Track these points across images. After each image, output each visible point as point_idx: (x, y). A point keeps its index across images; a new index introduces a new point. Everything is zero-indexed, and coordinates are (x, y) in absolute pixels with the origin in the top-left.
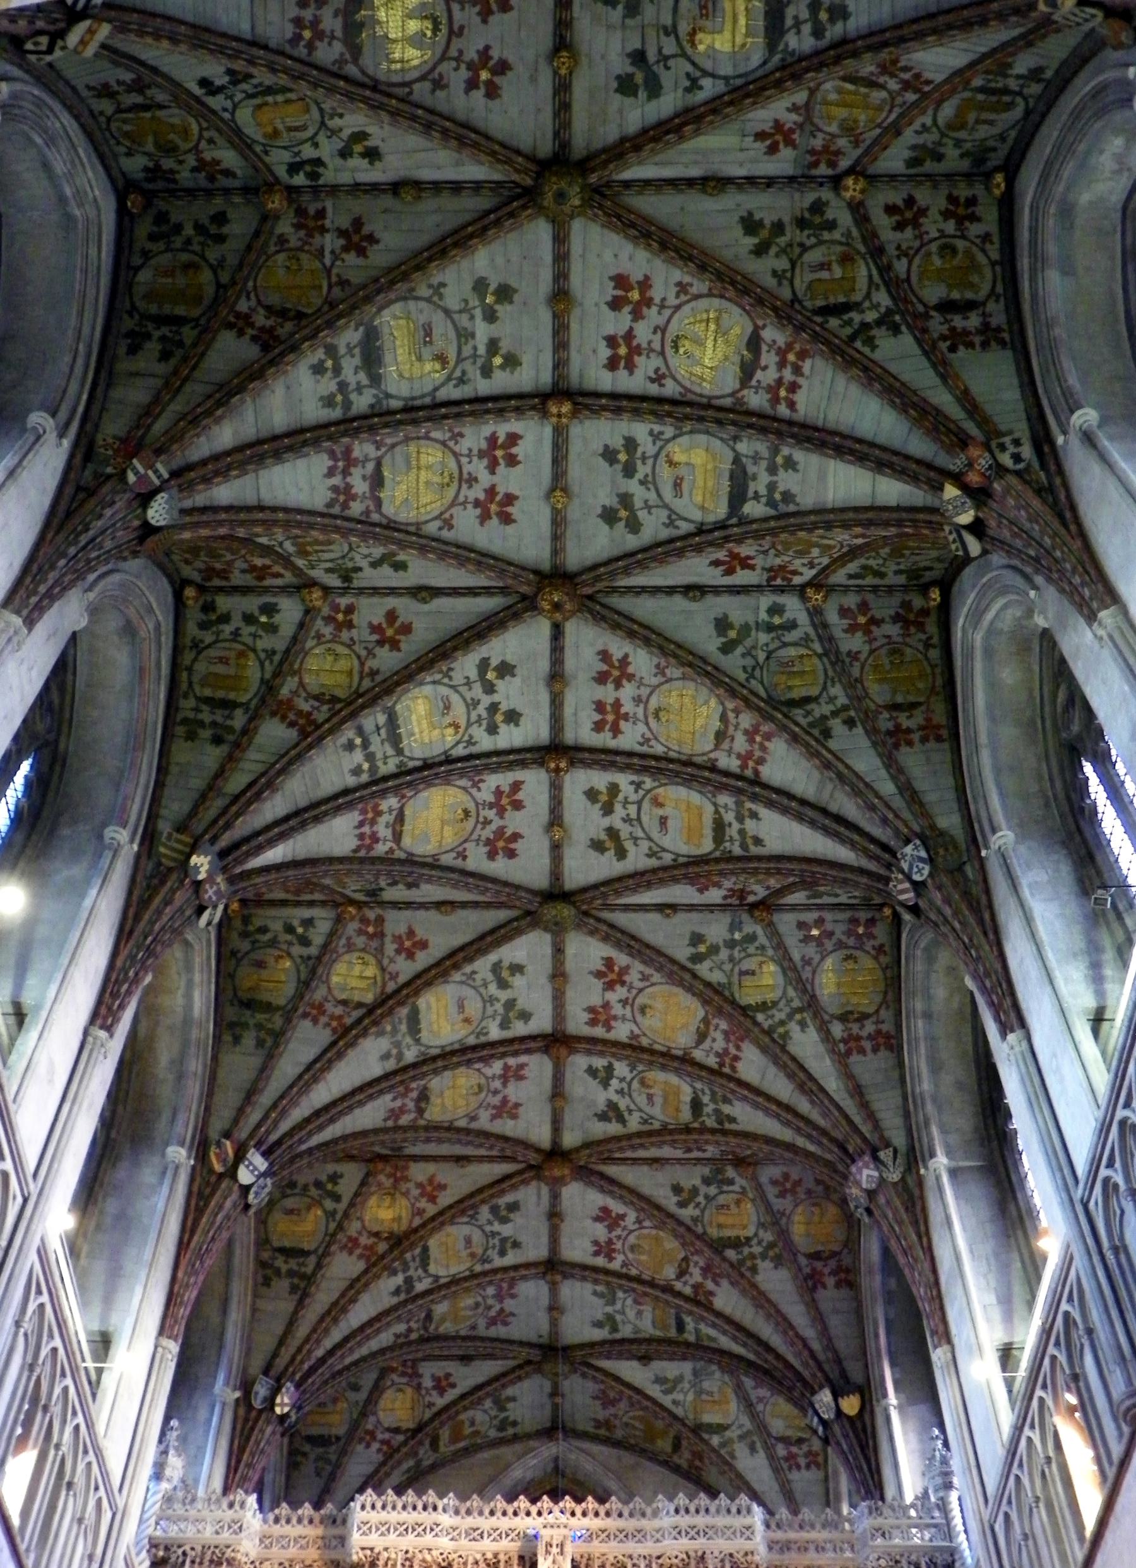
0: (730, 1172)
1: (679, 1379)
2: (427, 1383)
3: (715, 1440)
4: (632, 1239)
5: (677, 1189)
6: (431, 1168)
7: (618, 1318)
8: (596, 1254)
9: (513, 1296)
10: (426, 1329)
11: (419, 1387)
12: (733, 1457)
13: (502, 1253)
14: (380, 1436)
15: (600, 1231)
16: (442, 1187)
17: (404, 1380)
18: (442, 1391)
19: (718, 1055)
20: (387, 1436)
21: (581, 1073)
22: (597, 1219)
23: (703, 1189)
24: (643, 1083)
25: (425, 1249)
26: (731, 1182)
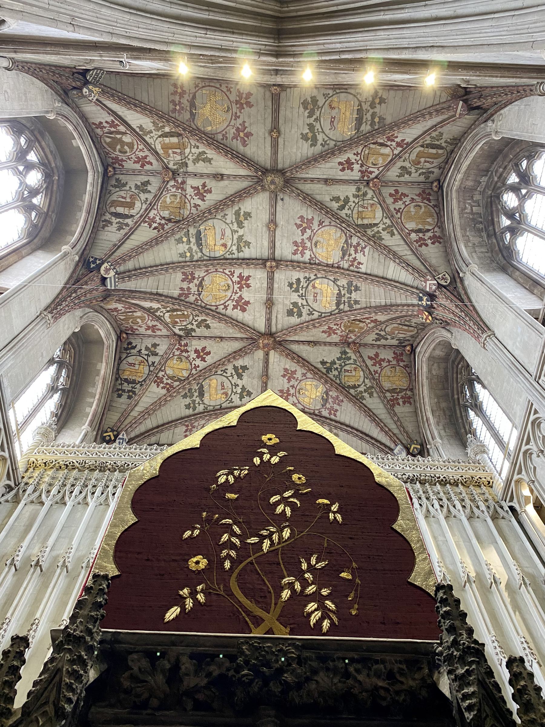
0: (181, 333)
1: (196, 161)
2: (356, 167)
3: (167, 129)
4: (229, 294)
5: (208, 327)
6: (328, 340)
7: (235, 227)
8: (248, 278)
9: (295, 243)
10: (346, 241)
11: (362, 166)
12: (153, 123)
13: (298, 280)
14: (394, 144)
15: (246, 295)
16: (323, 332)
17: (371, 169)
18: (348, 161)
20: (389, 143)
22: (247, 303)
23: (194, 327)
24: (226, 394)
25: (338, 304)
26: (180, 330)
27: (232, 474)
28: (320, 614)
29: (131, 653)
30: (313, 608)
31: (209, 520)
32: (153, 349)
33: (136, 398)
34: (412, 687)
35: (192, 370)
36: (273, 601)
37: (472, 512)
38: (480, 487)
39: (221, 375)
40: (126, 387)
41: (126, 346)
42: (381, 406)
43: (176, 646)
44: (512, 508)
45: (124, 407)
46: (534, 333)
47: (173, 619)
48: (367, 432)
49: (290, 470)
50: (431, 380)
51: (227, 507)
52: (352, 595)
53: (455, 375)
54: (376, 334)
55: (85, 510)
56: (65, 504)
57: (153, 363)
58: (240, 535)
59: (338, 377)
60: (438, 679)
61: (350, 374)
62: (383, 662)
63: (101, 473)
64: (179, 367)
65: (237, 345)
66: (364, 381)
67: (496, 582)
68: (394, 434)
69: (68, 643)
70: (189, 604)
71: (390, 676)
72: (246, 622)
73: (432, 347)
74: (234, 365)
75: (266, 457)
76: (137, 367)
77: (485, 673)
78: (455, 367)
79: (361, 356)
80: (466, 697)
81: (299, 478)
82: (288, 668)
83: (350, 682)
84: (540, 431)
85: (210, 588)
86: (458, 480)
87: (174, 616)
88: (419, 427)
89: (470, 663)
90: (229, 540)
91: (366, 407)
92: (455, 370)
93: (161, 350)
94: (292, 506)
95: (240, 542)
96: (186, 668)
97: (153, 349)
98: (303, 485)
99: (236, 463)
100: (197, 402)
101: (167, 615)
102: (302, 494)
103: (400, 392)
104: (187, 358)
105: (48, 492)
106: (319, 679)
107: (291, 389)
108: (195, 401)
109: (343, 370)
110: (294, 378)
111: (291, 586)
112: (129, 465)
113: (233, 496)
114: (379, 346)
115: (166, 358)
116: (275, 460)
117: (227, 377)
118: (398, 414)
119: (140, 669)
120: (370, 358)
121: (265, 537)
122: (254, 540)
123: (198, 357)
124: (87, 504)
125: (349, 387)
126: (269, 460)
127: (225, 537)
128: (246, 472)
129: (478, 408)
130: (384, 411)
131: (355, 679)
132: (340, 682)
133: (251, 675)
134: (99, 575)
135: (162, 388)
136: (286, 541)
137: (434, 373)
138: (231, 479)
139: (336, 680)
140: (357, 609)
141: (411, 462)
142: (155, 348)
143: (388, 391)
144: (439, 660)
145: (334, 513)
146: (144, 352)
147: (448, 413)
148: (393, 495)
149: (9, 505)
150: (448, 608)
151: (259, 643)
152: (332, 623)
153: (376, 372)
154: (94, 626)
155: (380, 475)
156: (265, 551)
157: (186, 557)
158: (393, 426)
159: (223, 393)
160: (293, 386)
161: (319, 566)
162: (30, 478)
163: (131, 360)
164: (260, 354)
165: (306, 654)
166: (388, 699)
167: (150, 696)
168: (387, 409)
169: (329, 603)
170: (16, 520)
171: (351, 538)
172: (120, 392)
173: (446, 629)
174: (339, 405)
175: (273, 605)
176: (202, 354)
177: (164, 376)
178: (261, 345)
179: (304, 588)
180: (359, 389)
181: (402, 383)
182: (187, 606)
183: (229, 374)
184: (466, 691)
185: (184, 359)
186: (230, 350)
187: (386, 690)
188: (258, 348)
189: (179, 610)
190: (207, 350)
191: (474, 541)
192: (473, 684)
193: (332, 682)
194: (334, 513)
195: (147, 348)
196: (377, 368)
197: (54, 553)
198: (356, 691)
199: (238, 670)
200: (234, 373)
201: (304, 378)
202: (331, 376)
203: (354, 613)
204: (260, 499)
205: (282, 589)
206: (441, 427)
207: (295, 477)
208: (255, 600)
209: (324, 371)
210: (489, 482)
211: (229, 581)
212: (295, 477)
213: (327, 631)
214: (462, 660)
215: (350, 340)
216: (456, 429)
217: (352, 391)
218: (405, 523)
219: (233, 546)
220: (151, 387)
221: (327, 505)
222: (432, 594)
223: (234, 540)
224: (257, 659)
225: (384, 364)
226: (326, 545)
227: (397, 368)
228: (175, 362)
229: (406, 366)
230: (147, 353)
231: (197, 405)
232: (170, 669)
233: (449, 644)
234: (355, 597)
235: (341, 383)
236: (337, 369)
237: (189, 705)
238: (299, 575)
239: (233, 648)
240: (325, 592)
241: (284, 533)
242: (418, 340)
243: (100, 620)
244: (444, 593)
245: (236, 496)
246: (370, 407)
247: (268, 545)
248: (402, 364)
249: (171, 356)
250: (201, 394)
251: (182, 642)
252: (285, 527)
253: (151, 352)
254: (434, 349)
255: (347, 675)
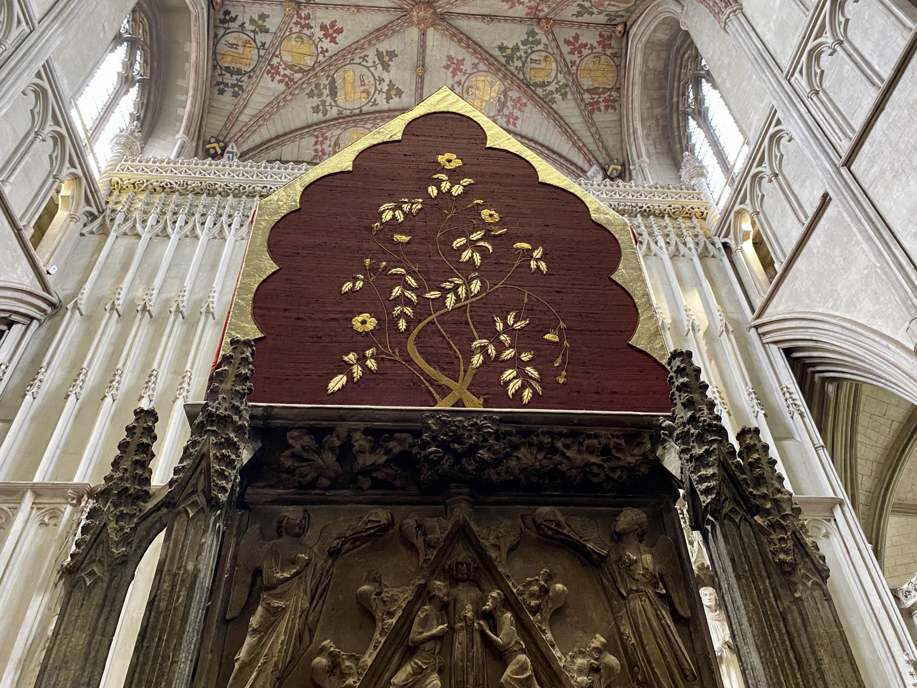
6: (511, 13)
19: (326, 138)
21: (406, 90)
24: (368, 93)
27: (401, 208)
28: (520, 382)
29: (290, 429)
30: (512, 376)
31: (373, 269)
32: (260, 22)
33: (245, 96)
34: (631, 463)
35: (318, 55)
36: (462, 368)
37: (677, 249)
38: (691, 218)
39: (360, 64)
40: (229, 79)
41: (222, 17)
42: (577, 112)
43: (345, 420)
44: (725, 245)
45: (230, 108)
46: (797, 8)
47: (339, 390)
48: (555, 148)
49: (478, 204)
50: (645, 75)
51: (397, 252)
52: (559, 360)
53: (677, 70)
54: (579, 5)
55: (195, 244)
56: (168, 237)
57: (263, 44)
58: (416, 288)
59: (519, 70)
60: (663, 455)
61: (538, 66)
62: (597, 436)
63: (210, 198)
64: (300, 51)
65: (380, 19)
66: (556, 77)
67: (693, 329)
68: (590, 151)
69: (212, 423)
70: (357, 371)
71: (605, 451)
72: (430, 392)
73: (652, 27)
74: (377, 51)
75: (445, 186)
76: (241, 49)
77: (728, 452)
78: (679, 57)
79: (555, 39)
80: (702, 479)
81: (491, 215)
82: (485, 444)
83: (557, 458)
84: (779, 148)
85: (383, 353)
86: (665, 210)
87: (339, 386)
88: (622, 141)
89: (711, 443)
90: (402, 294)
91: (556, 113)
92: (679, 62)
93: (273, 23)
94: (482, 251)
95: (417, 296)
96: (361, 445)
97: (260, 22)
98: (496, 224)
99: (404, 193)
100: (327, 104)
101: (331, 385)
102: (494, 236)
103: (603, 93)
104: (310, 37)
105: (144, 221)
106: (520, 455)
107: (456, 86)
108: (325, 101)
109: (529, 60)
110: (461, 70)
111: (483, 349)
112: (245, 188)
113: (404, 238)
114: (580, 24)
115: (281, 38)
116: (457, 190)
117: (368, 68)
118: (597, 124)
119: (303, 447)
120: (567, 42)
121: (448, 291)
122: (435, 294)
123: (326, 36)
124: (197, 237)
125: (535, 84)
126: (449, 190)
127: (397, 291)
128: (419, 206)
129: (701, 115)
130: (580, 119)
131: (563, 454)
132: (545, 458)
133: (438, 452)
134: (238, 341)
135: (280, 81)
136: (475, 296)
137: (651, 65)
138: (400, 216)
139: (540, 457)
140: (566, 377)
141: (609, 187)
142: (264, 21)
143: (587, 91)
144: (664, 434)
145: (537, 260)
146: (248, 27)
147: (662, 123)
148: (614, 237)
149: (95, 239)
150: (686, 379)
151: (448, 417)
152: (535, 393)
153: (573, 63)
154: (242, 403)
155: (597, 210)
156: (450, 308)
157: (349, 316)
158: (589, 140)
159: (363, 92)
160: (459, 83)
161: (518, 326)
162: (116, 203)
163: (231, 38)
164: (413, 33)
165: (504, 428)
166: (602, 476)
167: (319, 476)
168: (584, 117)
169: (530, 370)
170: (108, 256)
171: (558, 292)
172: (222, 86)
173: (682, 404)
174: (520, 110)
175: (462, 373)
176: (331, 31)
177: (279, 64)
178: (415, 19)
179: (499, 353)
180: (549, 88)
181: (607, 80)
182: (355, 375)
183: (370, 64)
184: (703, 472)
185: (306, 39)
186: (371, 25)
187: (600, 467)
188: (411, 23)
189: (345, 379)
190: (338, 25)
191: (675, 284)
192: (713, 465)
193: (536, 458)
194: (537, 260)
195: (252, 21)
196: (575, 57)
197: (164, 296)
198: (564, 468)
199: (424, 445)
200: (377, 62)
201: (475, 70)
202: (512, 68)
203: (561, 380)
204: (440, 243)
205: (472, 353)
206: (651, 142)
207: (485, 213)
208: (439, 366)
209: (503, 60)
210: (703, 213)
211: (406, 343)
212: (485, 213)
213: (529, 402)
214: (700, 439)
215: (541, 14)
216: (669, 144)
217: (539, 91)
218: (627, 273)
219: (408, 302)
220: (263, 80)
221: (528, 250)
222: (664, 362)
223: (408, 294)
224: (446, 434)
225: (586, 52)
226: (526, 300)
227: (603, 57)
228: (294, 43)
229: (614, 55)
230: (253, 28)
231: (328, 108)
232: (340, 447)
233: (685, 420)
234: (563, 362)
235: (525, 78)
236: (520, 58)
237: (366, 483)
238: (493, 336)
239: (416, 422)
240: (525, 357)
241: (473, 286)
242: (634, 16)
243: (248, 394)
244: (682, 361)
245: (407, 239)
246: (561, 112)
247: (453, 301)
248: (609, 52)
249: (288, 33)
250: (333, 93)
251: (352, 417)
252: (473, 278)
253: (258, 26)
254: (654, 31)
255: (553, 450)
